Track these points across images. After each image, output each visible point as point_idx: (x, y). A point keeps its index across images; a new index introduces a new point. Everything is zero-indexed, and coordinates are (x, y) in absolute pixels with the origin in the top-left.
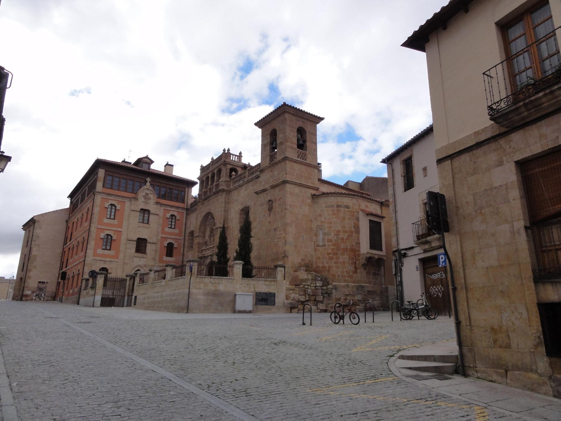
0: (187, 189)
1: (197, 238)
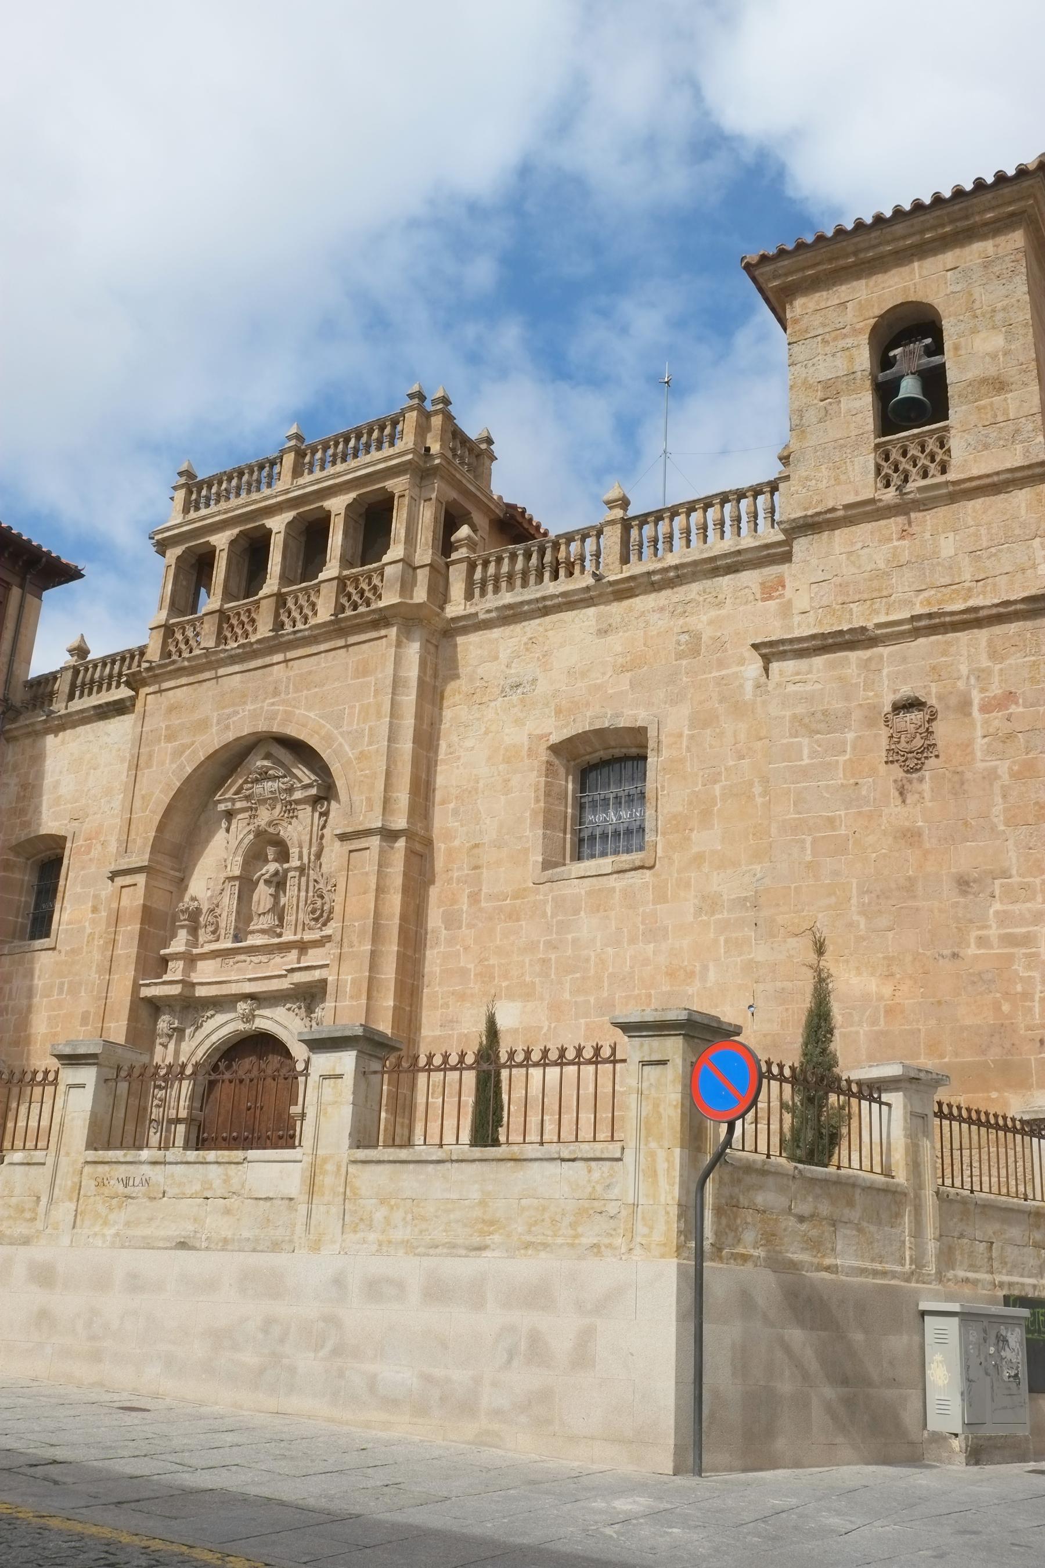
0: (16, 592)
1: (141, 879)
